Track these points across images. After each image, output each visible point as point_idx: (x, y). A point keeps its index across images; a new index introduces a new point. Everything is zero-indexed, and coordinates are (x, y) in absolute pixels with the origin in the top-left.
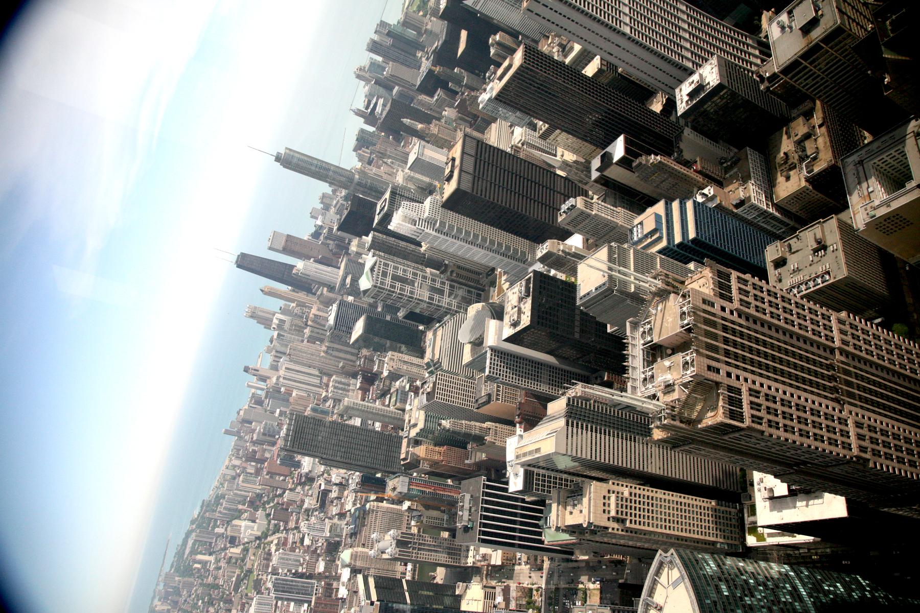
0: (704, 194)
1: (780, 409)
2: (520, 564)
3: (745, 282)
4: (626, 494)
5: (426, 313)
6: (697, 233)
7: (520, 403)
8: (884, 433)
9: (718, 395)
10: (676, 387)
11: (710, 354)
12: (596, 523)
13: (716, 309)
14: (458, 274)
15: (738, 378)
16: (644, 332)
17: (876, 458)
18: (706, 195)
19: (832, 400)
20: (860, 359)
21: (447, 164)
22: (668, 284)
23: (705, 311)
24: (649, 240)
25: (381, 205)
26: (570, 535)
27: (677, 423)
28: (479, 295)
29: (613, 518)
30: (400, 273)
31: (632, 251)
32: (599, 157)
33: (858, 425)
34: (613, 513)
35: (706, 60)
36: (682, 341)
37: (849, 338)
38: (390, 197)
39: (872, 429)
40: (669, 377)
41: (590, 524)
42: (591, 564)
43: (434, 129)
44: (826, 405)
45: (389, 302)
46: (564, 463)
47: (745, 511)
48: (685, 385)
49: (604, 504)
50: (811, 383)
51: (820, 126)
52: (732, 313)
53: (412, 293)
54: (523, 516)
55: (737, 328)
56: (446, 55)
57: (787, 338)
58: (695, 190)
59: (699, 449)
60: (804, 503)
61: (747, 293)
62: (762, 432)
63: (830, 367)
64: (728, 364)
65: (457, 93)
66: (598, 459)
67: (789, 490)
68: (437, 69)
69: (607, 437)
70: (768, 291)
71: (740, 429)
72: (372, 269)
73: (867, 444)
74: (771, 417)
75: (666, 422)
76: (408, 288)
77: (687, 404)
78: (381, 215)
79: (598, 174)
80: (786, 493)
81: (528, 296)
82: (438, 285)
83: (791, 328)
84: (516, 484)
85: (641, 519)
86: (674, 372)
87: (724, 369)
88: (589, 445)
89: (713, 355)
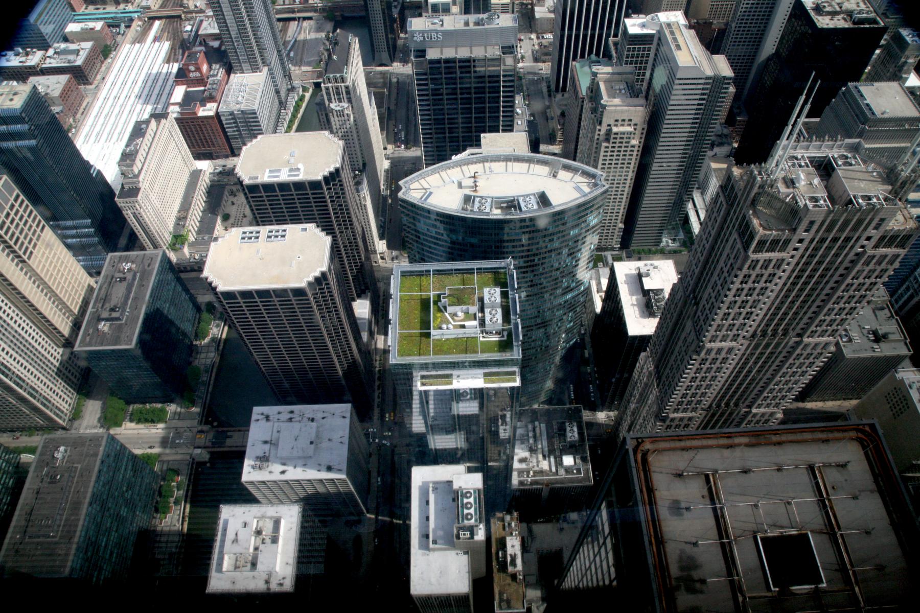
1: (758, 286)
2: (538, 38)
3: (891, 263)
4: (635, 142)
7: (712, 23)
8: (719, 370)
9: (783, 230)
10: (791, 190)
11: (826, 224)
12: (605, 114)
13: (871, 232)
15: (796, 249)
16: (847, 158)
17: (699, 361)
19: (755, 331)
20: (786, 358)
22: (904, 184)
26: (589, 88)
27: (755, 190)
29: (610, 130)
33: (730, 350)
34: (615, 129)
37: (808, 351)
39: (724, 360)
40: (802, 183)
41: (604, 107)
42: (548, 111)
44: (752, 325)
46: (660, 78)
47: (617, 253)
48: (794, 198)
49: (624, 120)
52: (863, 247)
54: (592, 36)
55: (845, 252)
57: (822, 297)
59: (719, 211)
60: (635, 303)
61: (879, 263)
62: (740, 269)
63: (785, 333)
64: (812, 241)
66: (669, 112)
67: (649, 291)
69: (691, 121)
70: (875, 283)
71: (746, 247)
73: (713, 355)
74: (753, 278)
75: (759, 179)
77: (775, 198)
80: (646, 287)
83: (833, 301)
84: (634, 25)
85: (609, 158)
86: (807, 188)
88: (680, 103)
89: (825, 227)
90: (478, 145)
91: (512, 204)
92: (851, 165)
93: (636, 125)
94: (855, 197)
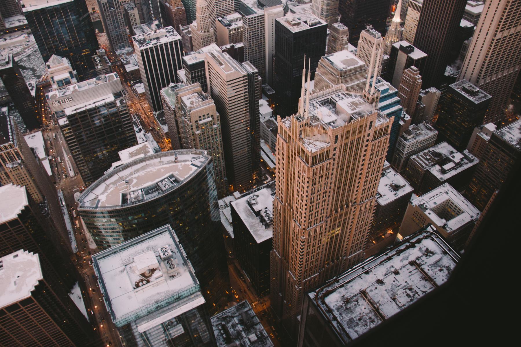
0: (405, 115)
11: (344, 134)
13: (368, 131)
18: (404, 117)
23: (366, 124)
32: (409, 44)
49: (204, 116)
50: (338, 196)
79: (398, 47)
80: (256, 211)
81: (310, 26)
84: (190, 59)
87: (337, 145)
90: (119, 159)
91: (156, 188)
93: (212, 116)
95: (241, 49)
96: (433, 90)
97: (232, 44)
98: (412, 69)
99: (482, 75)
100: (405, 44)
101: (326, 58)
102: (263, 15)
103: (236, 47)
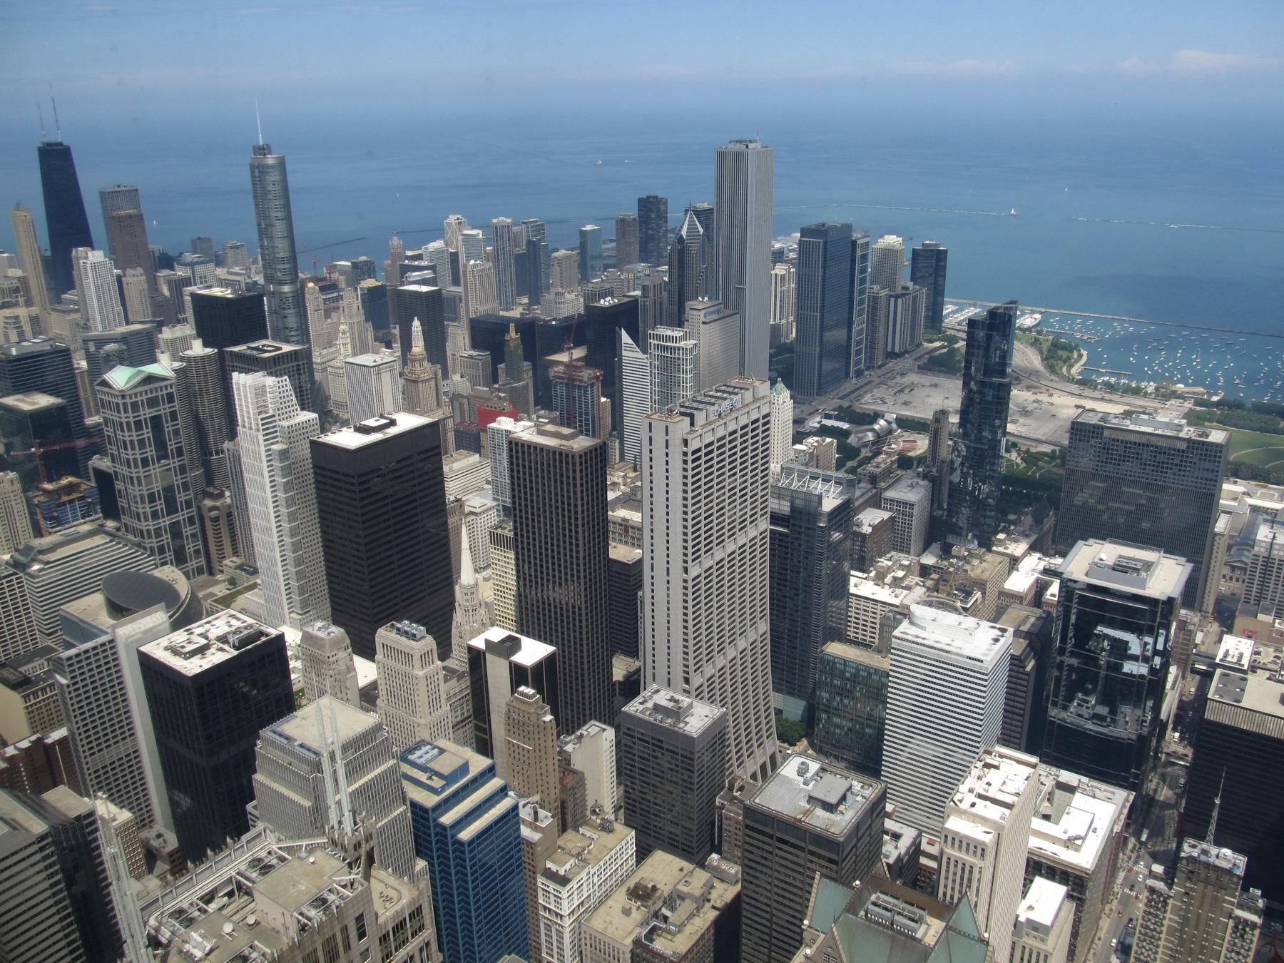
0: (536, 813)
5: (122, 502)
6: (471, 842)
13: (358, 945)
14: (215, 520)
16: (260, 860)
18: (536, 819)
21: (382, 416)
22: (357, 846)
24: (422, 777)
25: (269, 346)
28: (200, 571)
30: (168, 427)
31: (392, 762)
32: (507, 633)
35: (711, 700)
36: (281, 928)
38: (287, 353)
43: (425, 369)
45: (109, 432)
51: (713, 907)
53: (145, 462)
56: (540, 340)
58: (537, 798)
65: (496, 381)
68: (513, 335)
72: (150, 379)
76: (151, 452)
78: (249, 352)
81: (237, 649)
82: (181, 497)
92: (272, 866)
94: (301, 914)
95: (62, 742)
96: (592, 728)
97: (34, 738)
98: (522, 694)
99: (691, 662)
100: (497, 634)
101: (274, 732)
102: (111, 642)
103: (49, 741)
